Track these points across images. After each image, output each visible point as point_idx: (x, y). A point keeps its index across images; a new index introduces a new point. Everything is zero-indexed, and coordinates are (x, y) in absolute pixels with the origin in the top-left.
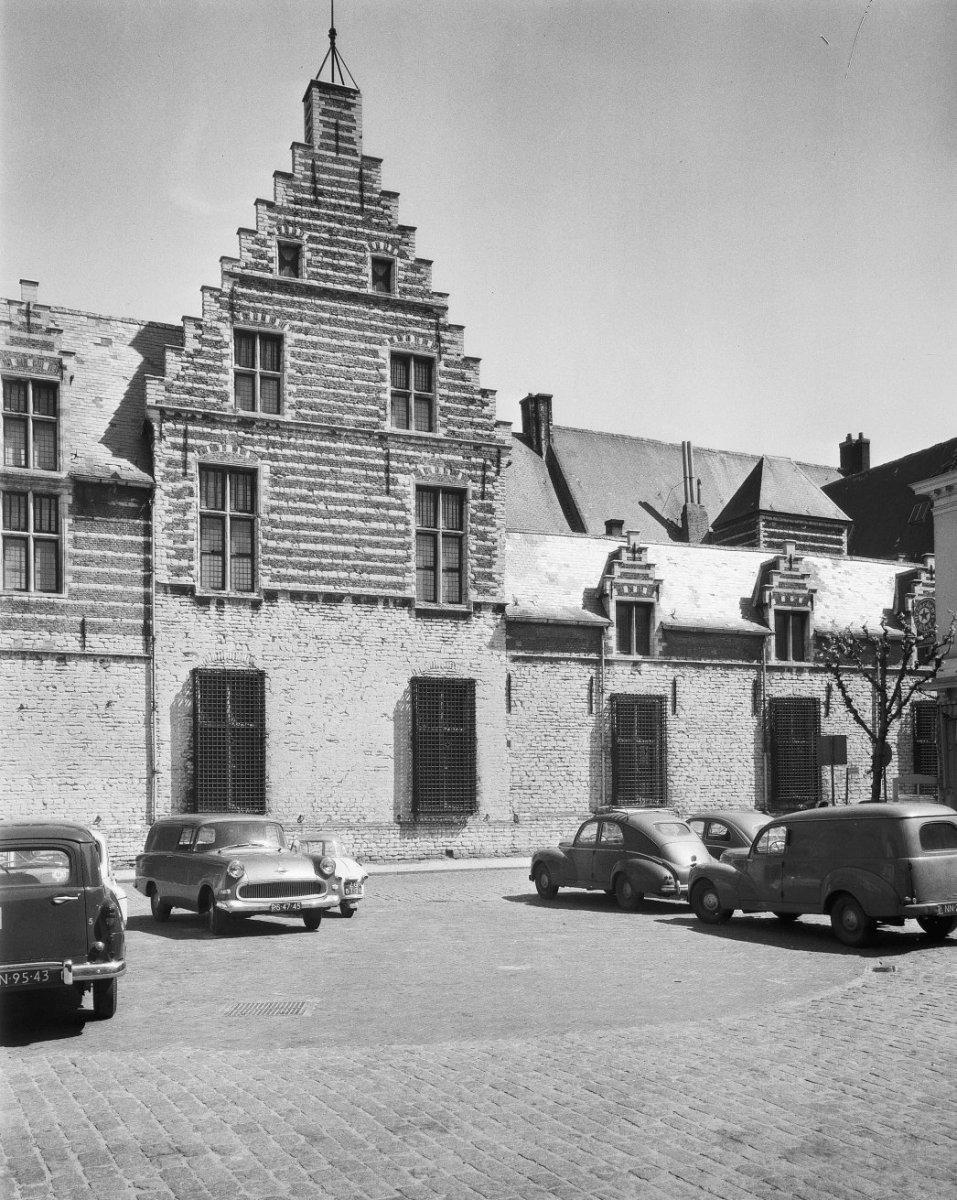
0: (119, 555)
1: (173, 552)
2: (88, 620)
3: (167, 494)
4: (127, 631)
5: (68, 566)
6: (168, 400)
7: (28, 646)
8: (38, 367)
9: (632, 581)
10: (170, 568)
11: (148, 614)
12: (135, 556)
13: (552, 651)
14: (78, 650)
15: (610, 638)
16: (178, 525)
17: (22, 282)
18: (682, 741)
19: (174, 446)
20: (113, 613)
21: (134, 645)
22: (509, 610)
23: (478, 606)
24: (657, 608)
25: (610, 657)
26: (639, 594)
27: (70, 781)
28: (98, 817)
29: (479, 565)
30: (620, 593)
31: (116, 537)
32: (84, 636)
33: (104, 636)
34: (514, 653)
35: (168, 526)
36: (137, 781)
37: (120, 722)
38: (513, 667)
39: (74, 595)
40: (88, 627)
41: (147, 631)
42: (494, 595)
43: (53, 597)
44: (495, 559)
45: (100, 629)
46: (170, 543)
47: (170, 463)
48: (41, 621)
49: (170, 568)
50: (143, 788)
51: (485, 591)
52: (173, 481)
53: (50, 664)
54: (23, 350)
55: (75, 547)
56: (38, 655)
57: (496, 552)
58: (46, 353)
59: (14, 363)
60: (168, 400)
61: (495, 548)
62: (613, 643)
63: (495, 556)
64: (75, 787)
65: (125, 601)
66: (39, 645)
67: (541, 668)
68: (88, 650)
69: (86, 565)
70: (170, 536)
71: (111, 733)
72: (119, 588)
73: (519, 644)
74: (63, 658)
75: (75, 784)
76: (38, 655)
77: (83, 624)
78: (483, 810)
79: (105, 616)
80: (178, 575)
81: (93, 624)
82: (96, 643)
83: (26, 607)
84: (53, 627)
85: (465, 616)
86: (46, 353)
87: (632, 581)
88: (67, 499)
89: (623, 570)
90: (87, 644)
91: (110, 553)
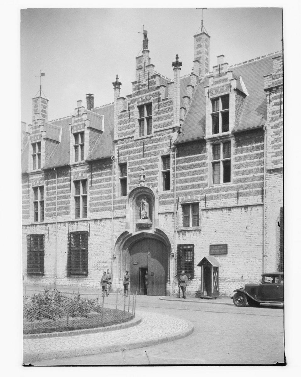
0: (252, 161)
1: (274, 154)
2: (239, 191)
3: (272, 128)
4: (255, 193)
5: (233, 170)
6: (273, 83)
7: (218, 206)
8: (222, 91)
10: (273, 162)
11: (262, 185)
12: (258, 159)
14: (236, 205)
16: (276, 141)
17: (218, 57)
19: (276, 104)
20: (249, 187)
21: (257, 199)
27: (232, 260)
28: (242, 276)
31: (251, 153)
32: (238, 199)
33: (246, 197)
35: (273, 142)
36: (257, 260)
37: (251, 235)
39: (235, 182)
40: (240, 195)
41: (262, 192)
43: (227, 185)
45: (244, 195)
46: (273, 150)
47: (274, 113)
48: (223, 195)
49: (273, 162)
50: (261, 263)
52: (275, 121)
53: (225, 211)
54: (217, 85)
55: (236, 161)
56: (221, 209)
58: (225, 83)
59: (214, 92)
60: (273, 83)
64: (234, 263)
65: (254, 181)
66: (222, 205)
68: (239, 205)
69: (239, 168)
70: (273, 147)
71: (247, 239)
72: (251, 175)
74: (230, 208)
75: (234, 262)
76: (221, 209)
77: (238, 194)
79: (246, 189)
80: (276, 164)
81: (241, 193)
82: (243, 201)
83: (218, 190)
84: (226, 196)
86: (225, 83)
88: (233, 141)
90: (239, 202)
91: (248, 161)
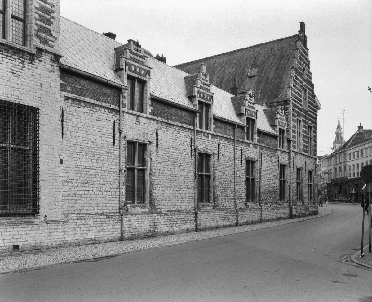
9: (136, 64)
13: (91, 98)
15: (124, 98)
18: (157, 164)
22: (61, 60)
23: (40, 50)
24: (147, 84)
25: (124, 109)
26: (139, 73)
29: (41, 20)
30: (130, 70)
34: (66, 94)
38: (64, 105)
42: (52, 47)
44: (52, 20)
51: (45, 42)
57: (52, 15)
61: (53, 12)
62: (126, 101)
63: (53, 18)
67: (84, 110)
73: (69, 88)
78: (43, 211)
85: (32, 57)
87: (136, 64)
89: (132, 56)
